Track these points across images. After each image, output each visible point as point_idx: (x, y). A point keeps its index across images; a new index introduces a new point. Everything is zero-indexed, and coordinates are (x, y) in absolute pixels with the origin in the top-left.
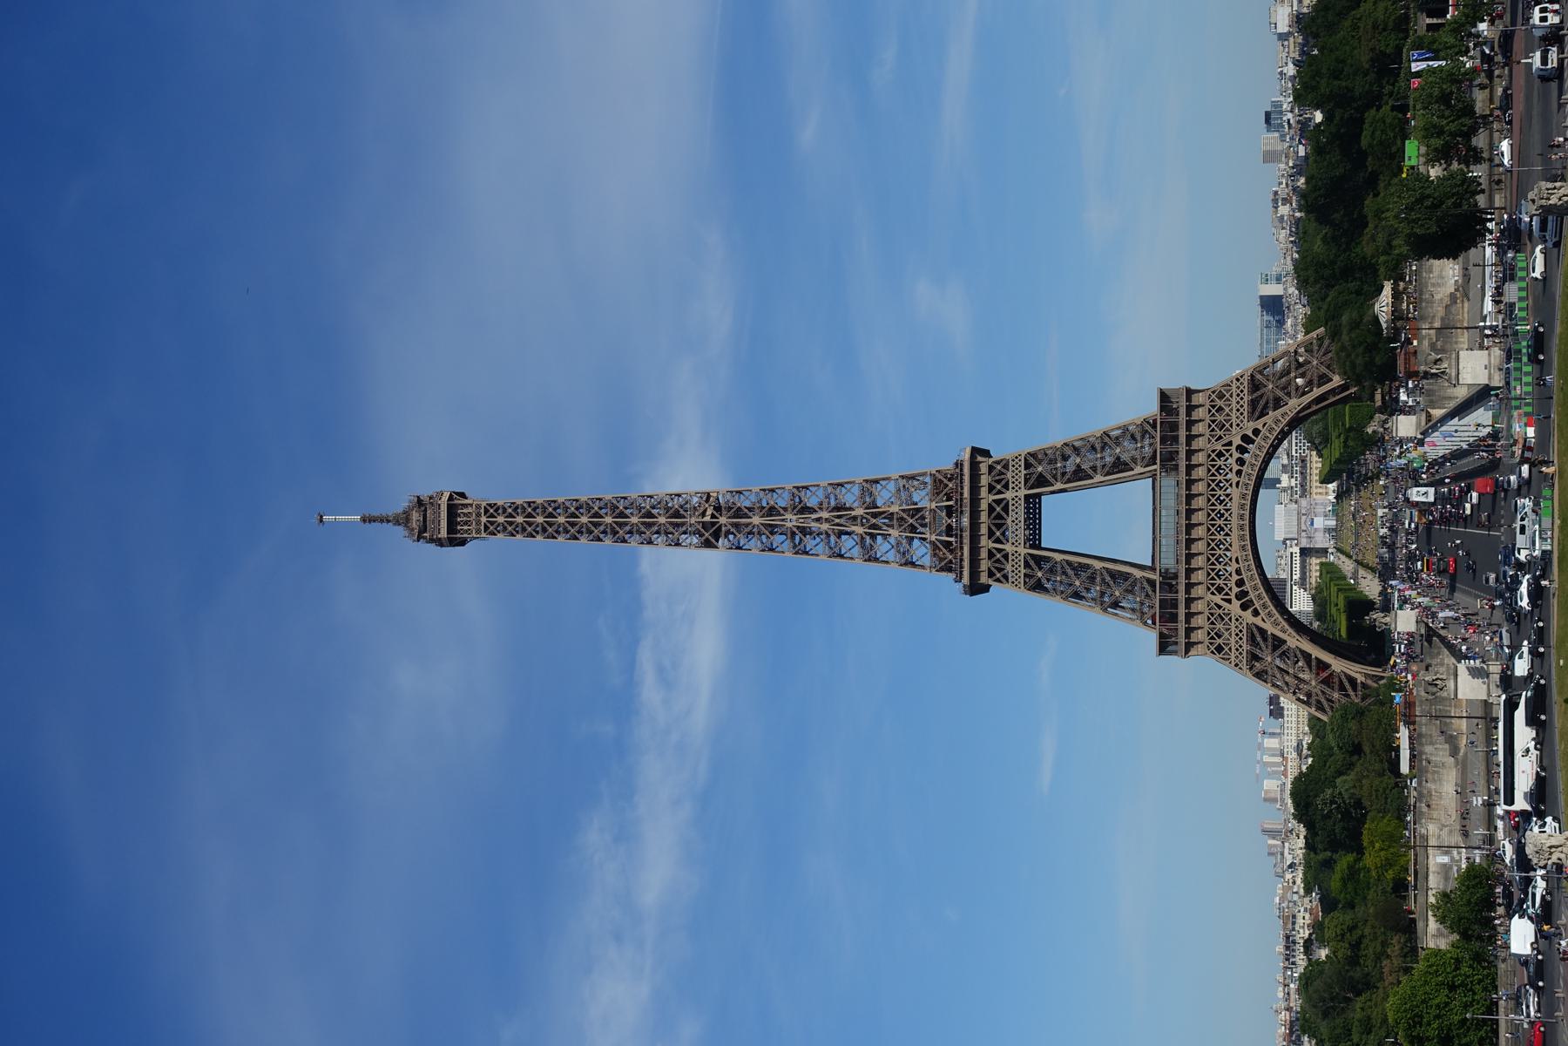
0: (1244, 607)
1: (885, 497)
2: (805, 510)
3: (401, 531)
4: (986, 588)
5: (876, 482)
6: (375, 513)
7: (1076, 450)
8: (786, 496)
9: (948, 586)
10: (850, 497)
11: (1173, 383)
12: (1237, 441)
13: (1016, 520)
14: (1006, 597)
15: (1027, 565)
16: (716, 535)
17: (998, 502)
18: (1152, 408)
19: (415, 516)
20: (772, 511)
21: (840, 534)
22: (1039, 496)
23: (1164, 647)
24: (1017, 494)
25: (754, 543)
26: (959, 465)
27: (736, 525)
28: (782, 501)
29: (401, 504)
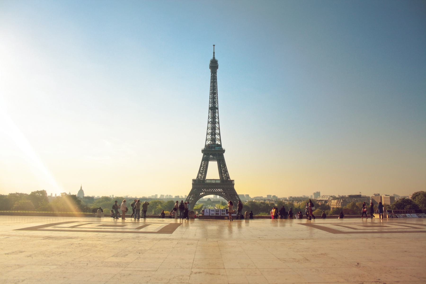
1: (217, 137)
2: (216, 123)
3: (212, 58)
5: (220, 135)
7: (224, 167)
8: (217, 121)
9: (203, 147)
10: (217, 131)
11: (235, 183)
12: (226, 192)
14: (201, 155)
16: (211, 110)
18: (231, 179)
22: (217, 161)
23: (194, 180)
26: (222, 149)
28: (217, 120)
29: (216, 58)
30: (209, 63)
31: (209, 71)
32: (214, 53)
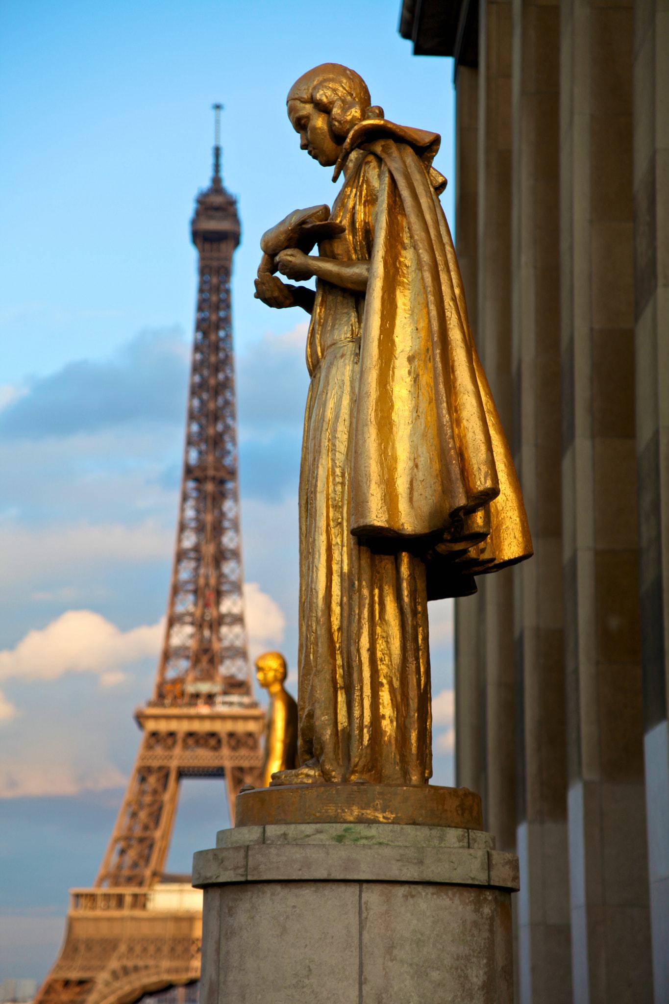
0: (115, 975)
3: (205, 183)
4: (141, 726)
6: (224, 160)
13: (204, 757)
15: (160, 768)
16: (197, 480)
17: (219, 742)
19: (217, 200)
20: (218, 530)
21: (195, 592)
24: (226, 758)
25: (190, 513)
27: (205, 498)
28: (228, 540)
29: (230, 184)
30: (189, 209)
31: (190, 256)
32: (217, 152)
